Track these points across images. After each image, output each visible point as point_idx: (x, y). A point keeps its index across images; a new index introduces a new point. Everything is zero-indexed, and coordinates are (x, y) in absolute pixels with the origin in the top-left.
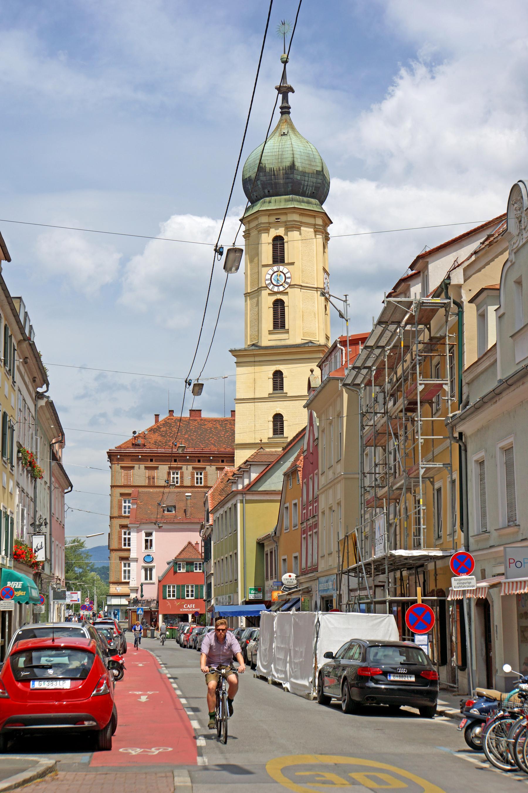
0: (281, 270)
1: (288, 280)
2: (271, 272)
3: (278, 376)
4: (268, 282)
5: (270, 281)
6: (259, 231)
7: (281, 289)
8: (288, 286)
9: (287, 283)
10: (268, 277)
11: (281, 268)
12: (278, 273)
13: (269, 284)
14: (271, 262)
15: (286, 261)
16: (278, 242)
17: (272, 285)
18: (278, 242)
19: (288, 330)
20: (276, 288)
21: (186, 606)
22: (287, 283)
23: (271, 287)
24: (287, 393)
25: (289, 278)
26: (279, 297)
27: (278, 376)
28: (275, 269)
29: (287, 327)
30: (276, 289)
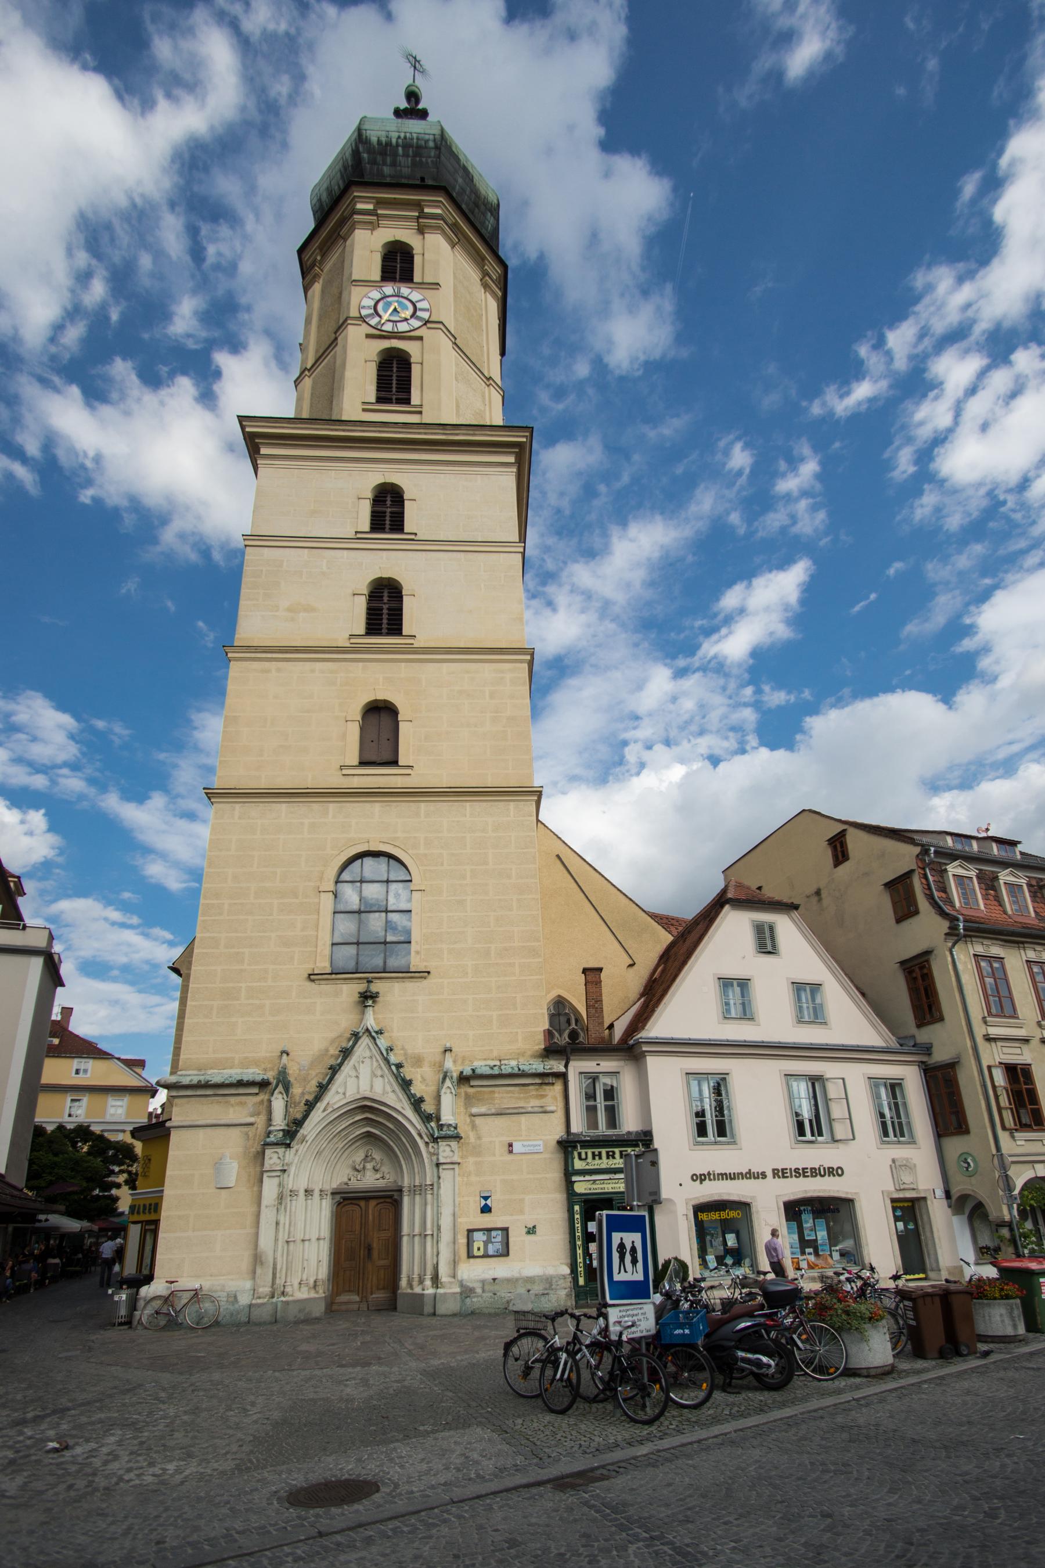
2: (376, 295)
5: (372, 311)
9: (419, 318)
11: (405, 290)
14: (376, 275)
15: (415, 281)
22: (419, 318)
28: (389, 289)
29: (415, 399)
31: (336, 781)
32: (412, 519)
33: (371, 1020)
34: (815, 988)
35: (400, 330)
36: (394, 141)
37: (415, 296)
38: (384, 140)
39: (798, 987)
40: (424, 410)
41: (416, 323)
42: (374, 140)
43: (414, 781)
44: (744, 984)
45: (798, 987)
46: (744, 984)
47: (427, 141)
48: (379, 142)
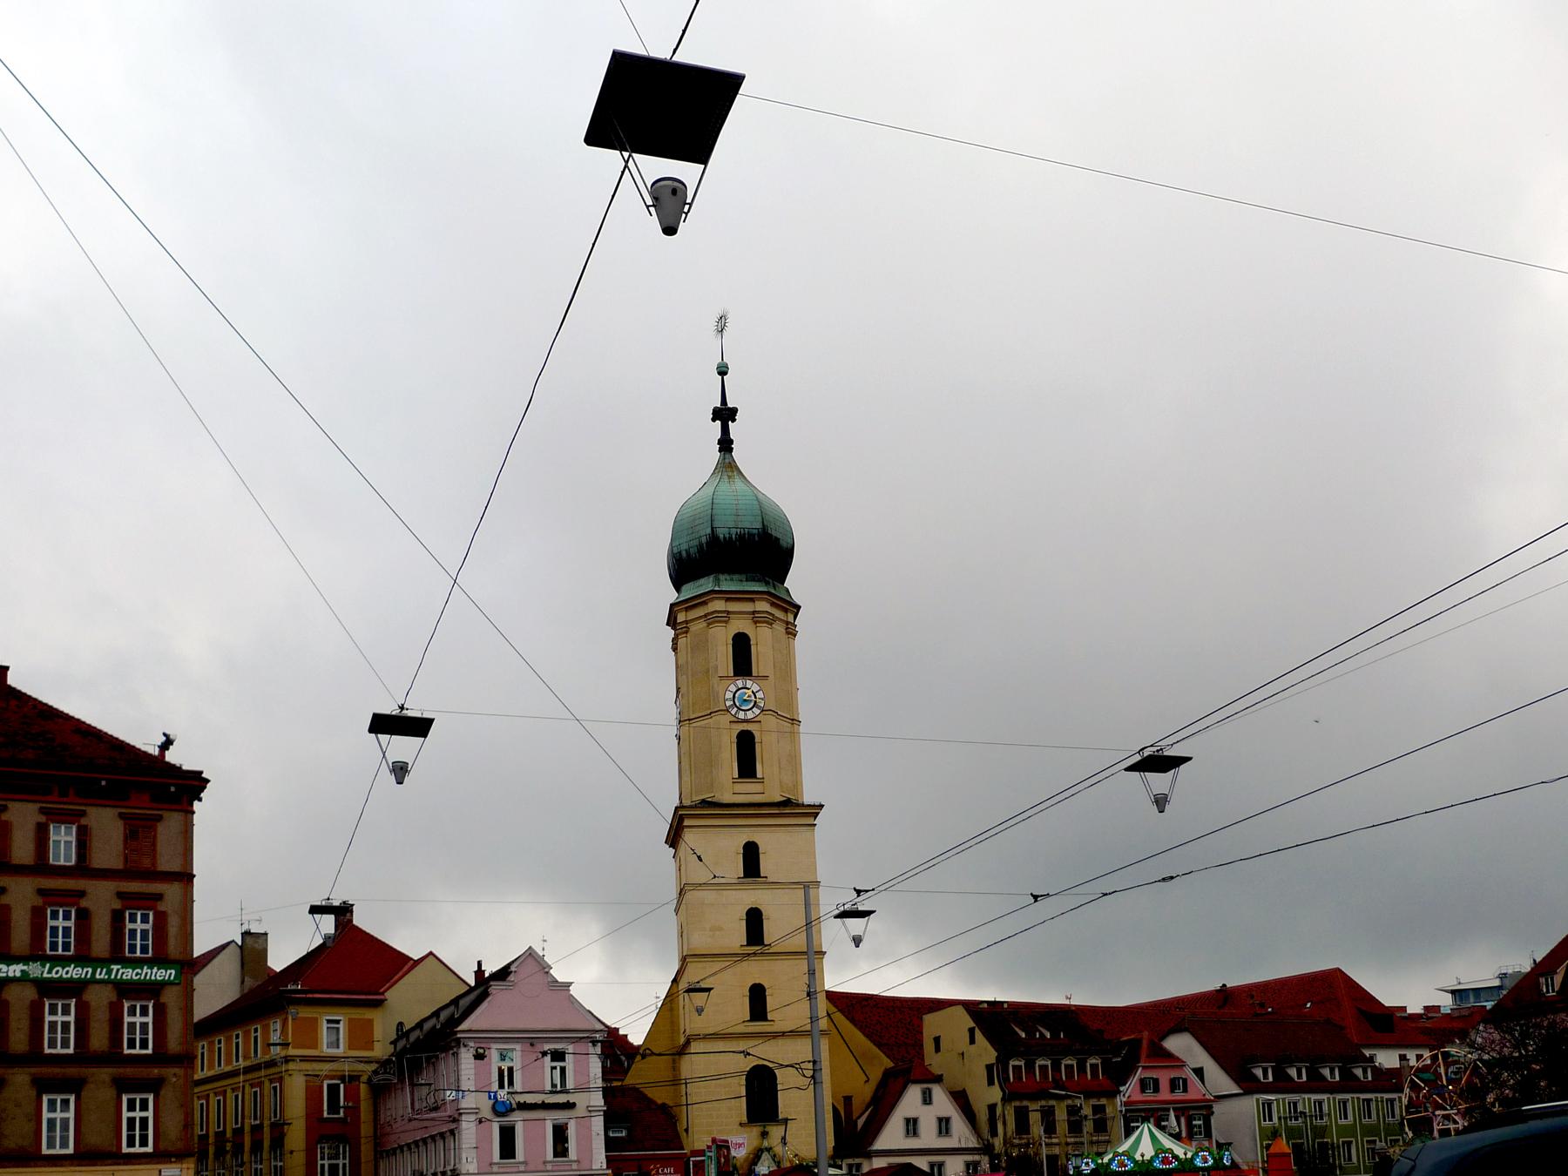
4: (729, 703)
5: (732, 703)
6: (709, 624)
7: (750, 715)
8: (759, 711)
10: (729, 695)
11: (749, 684)
12: (747, 691)
16: (742, 646)
17: (735, 709)
18: (742, 646)
19: (763, 778)
21: (662, 1171)
22: (758, 707)
24: (766, 877)
28: (740, 683)
29: (759, 775)
30: (741, 715)
31: (741, 1029)
32: (766, 866)
33: (766, 1144)
34: (948, 1120)
36: (734, 536)
38: (727, 536)
39: (940, 1120)
40: (765, 781)
41: (757, 711)
42: (722, 536)
43: (777, 1027)
44: (915, 1121)
45: (940, 1120)
46: (915, 1121)
47: (754, 535)
48: (725, 538)
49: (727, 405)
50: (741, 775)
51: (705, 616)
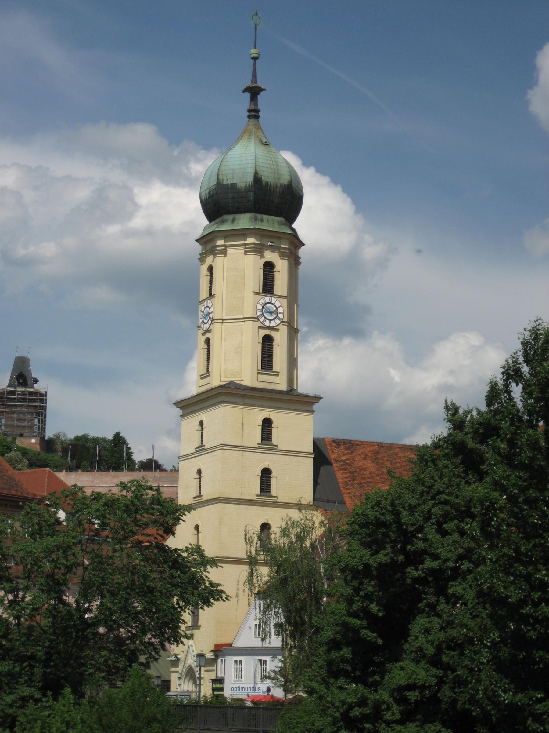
0: (273, 302)
1: (280, 316)
3: (267, 423)
4: (259, 313)
7: (273, 324)
9: (279, 319)
10: (260, 307)
11: (274, 300)
13: (260, 316)
17: (263, 318)
20: (267, 322)
23: (262, 319)
25: (281, 313)
26: (268, 332)
27: (267, 423)
28: (267, 299)
30: (267, 323)
35: (272, 326)
37: (278, 304)
49: (256, 83)
50: (263, 368)
51: (245, 245)
